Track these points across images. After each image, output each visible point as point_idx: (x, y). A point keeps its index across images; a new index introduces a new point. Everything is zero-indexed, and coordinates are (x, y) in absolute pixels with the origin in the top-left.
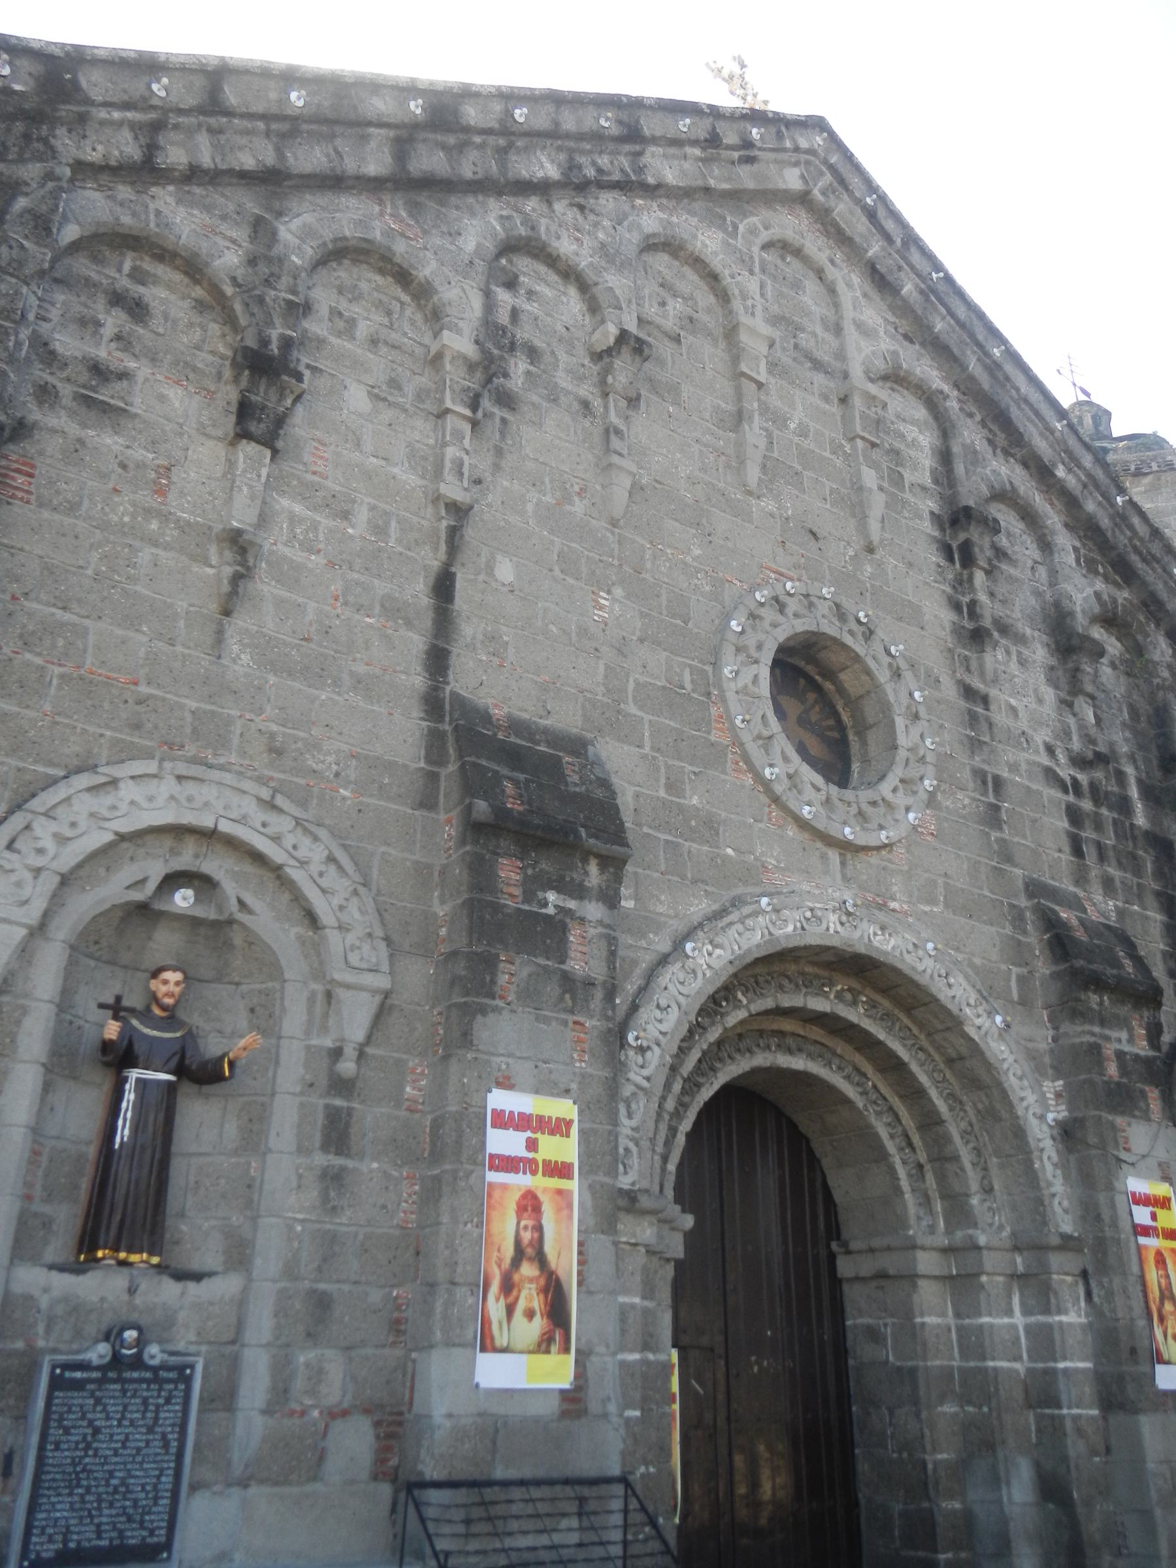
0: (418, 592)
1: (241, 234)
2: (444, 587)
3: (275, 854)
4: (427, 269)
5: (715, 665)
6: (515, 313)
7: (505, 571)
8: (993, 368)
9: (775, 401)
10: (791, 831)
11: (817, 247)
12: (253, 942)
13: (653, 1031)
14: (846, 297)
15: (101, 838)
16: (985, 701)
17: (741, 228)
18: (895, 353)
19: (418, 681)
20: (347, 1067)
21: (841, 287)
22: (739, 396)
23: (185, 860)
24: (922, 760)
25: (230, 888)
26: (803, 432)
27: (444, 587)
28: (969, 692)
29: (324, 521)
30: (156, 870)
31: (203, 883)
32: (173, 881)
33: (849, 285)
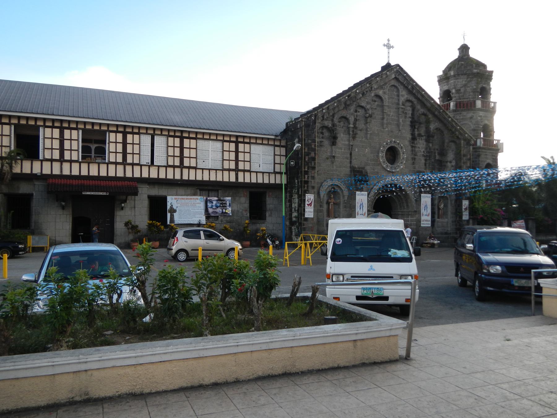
0: (349, 156)
1: (331, 122)
2: (351, 154)
3: (339, 185)
4: (348, 117)
5: (379, 154)
6: (357, 115)
7: (357, 150)
8: (422, 96)
9: (389, 113)
10: (386, 172)
11: (397, 84)
12: (338, 192)
13: (371, 195)
14: (400, 90)
15: (327, 186)
16: (415, 147)
17: (385, 87)
18: (407, 97)
19: (349, 165)
20: (346, 202)
21: (400, 89)
22: (383, 115)
23: (332, 187)
24: (404, 159)
25: (336, 188)
26: (392, 116)
27: (351, 154)
28: (412, 147)
29: (340, 151)
30: (330, 188)
31: (334, 188)
32: (332, 188)
33: (401, 88)
